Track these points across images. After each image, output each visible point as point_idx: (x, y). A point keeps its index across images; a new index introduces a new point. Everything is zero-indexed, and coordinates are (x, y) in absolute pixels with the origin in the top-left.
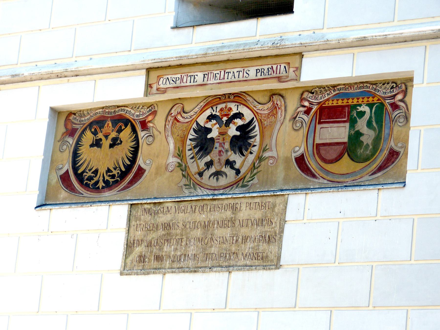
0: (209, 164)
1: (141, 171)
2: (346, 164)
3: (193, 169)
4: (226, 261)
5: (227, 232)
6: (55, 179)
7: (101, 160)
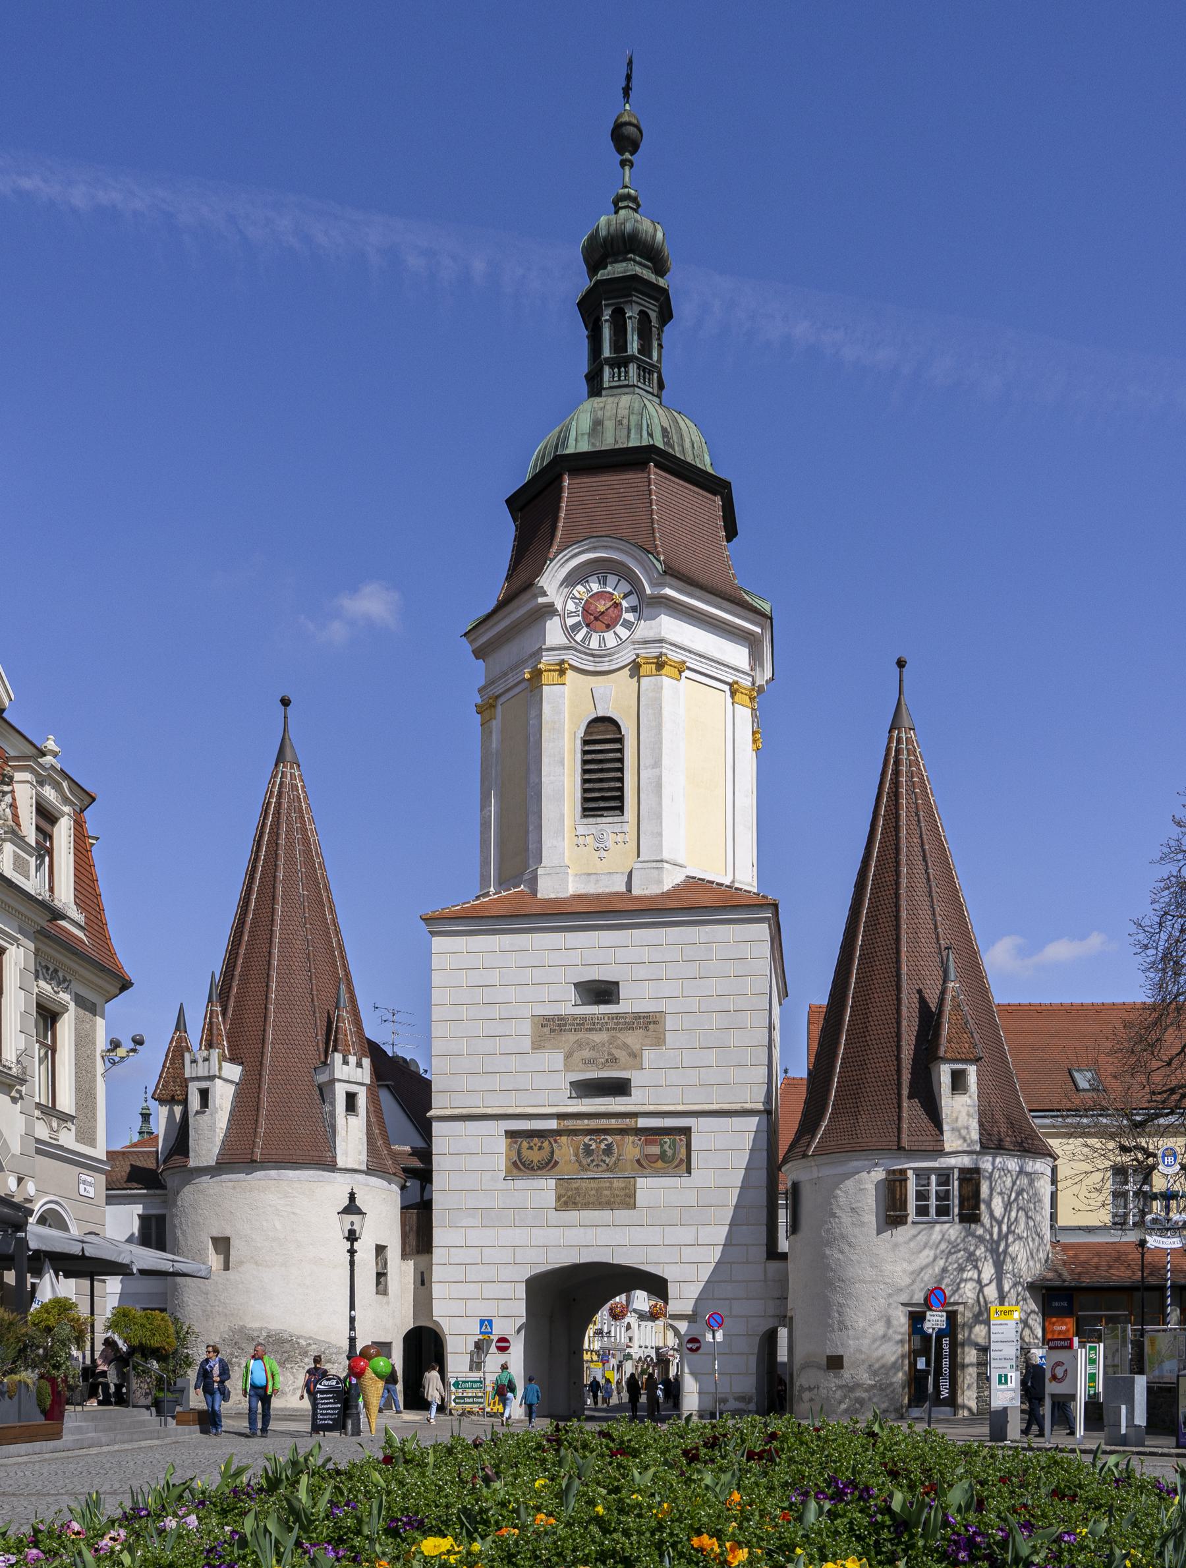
0: (592, 1161)
1: (556, 1163)
2: (660, 1164)
3: (584, 1162)
4: (609, 1205)
5: (607, 1193)
6: (509, 1164)
7: (535, 1156)
